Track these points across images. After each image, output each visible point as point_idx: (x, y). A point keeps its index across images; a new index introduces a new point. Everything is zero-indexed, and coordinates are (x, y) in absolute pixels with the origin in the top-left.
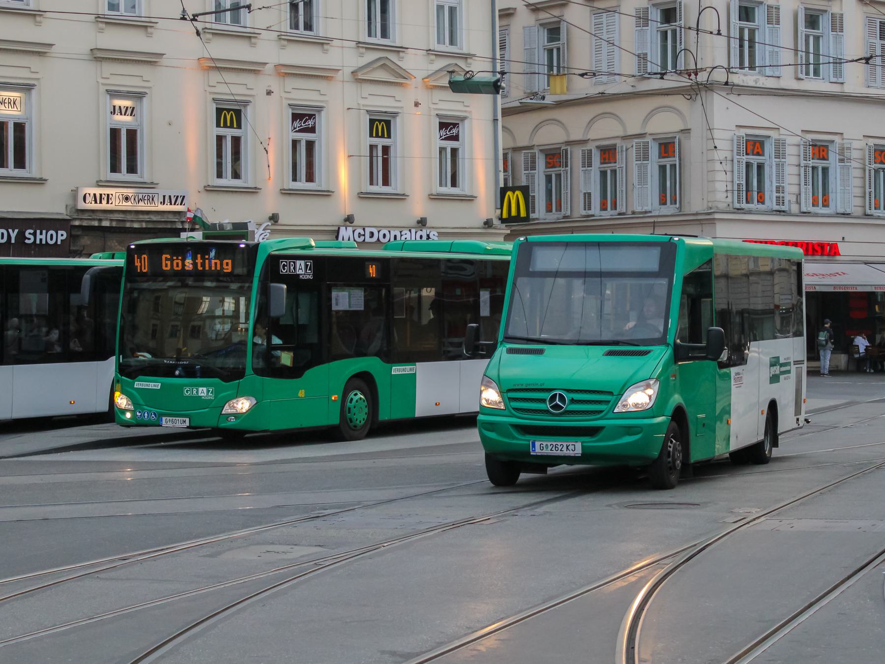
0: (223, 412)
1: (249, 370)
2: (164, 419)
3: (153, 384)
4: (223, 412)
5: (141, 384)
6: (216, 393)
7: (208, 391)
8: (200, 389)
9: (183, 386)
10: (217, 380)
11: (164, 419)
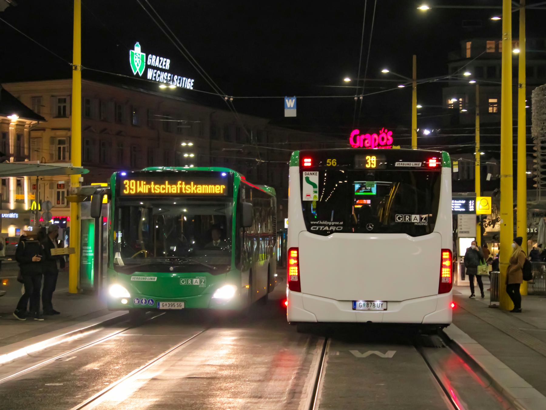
3: (151, 278)
7: (201, 282)
8: (194, 280)
11: (161, 304)
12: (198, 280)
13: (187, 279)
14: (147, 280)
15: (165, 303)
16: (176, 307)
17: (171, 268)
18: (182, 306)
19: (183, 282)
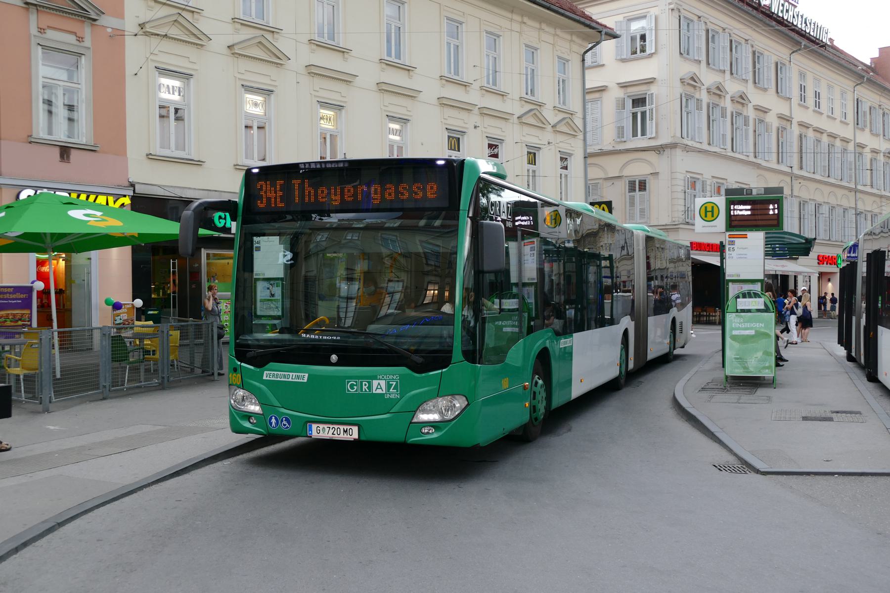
0: (415, 420)
1: (457, 354)
2: (314, 426)
3: (296, 375)
4: (415, 420)
5: (275, 373)
6: (404, 386)
7: (389, 386)
8: (375, 383)
9: (343, 379)
10: (404, 370)
12: (383, 383)
13: (359, 381)
14: (290, 380)
15: (321, 426)
16: (343, 437)
17: (334, 358)
18: (354, 434)
19: (352, 388)
